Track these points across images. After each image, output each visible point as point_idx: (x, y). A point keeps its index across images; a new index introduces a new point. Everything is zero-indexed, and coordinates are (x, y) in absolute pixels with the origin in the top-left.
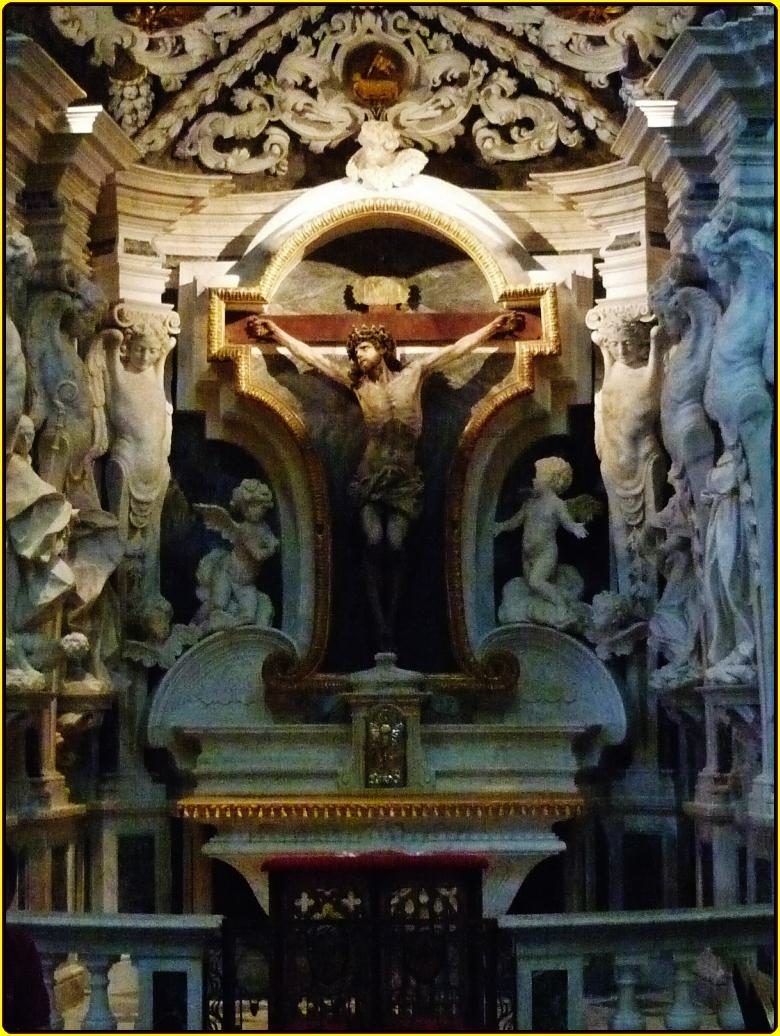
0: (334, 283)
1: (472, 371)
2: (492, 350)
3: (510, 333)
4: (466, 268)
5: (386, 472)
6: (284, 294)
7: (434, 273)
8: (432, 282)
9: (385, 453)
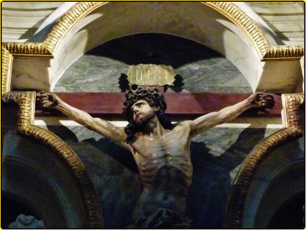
0: (110, 71)
1: (230, 142)
2: (246, 126)
3: (262, 108)
4: (220, 63)
5: (161, 213)
6: (68, 80)
7: (195, 67)
8: (193, 73)
9: (160, 197)
